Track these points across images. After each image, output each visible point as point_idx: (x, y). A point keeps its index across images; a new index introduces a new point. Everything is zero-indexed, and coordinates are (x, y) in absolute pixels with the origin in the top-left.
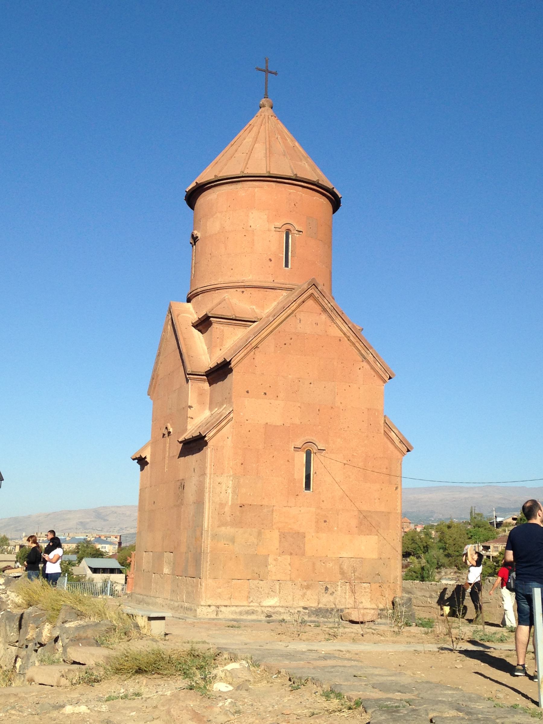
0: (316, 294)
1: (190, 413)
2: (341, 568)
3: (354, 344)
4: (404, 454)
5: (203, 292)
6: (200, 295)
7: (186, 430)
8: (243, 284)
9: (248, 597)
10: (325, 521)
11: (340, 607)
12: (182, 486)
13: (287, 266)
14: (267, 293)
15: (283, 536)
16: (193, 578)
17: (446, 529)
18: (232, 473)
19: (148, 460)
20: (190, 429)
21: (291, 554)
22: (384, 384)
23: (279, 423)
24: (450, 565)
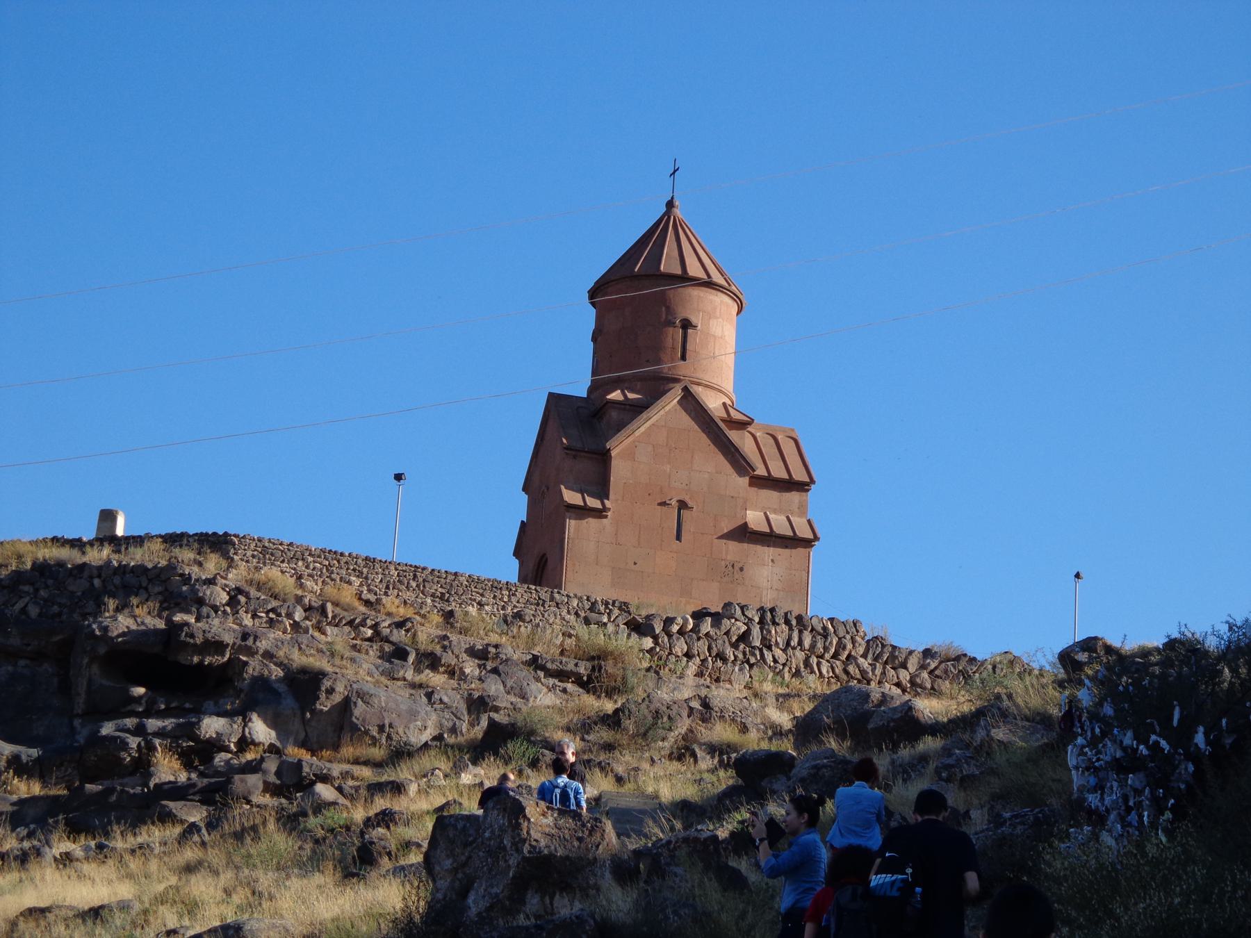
5: (707, 386)
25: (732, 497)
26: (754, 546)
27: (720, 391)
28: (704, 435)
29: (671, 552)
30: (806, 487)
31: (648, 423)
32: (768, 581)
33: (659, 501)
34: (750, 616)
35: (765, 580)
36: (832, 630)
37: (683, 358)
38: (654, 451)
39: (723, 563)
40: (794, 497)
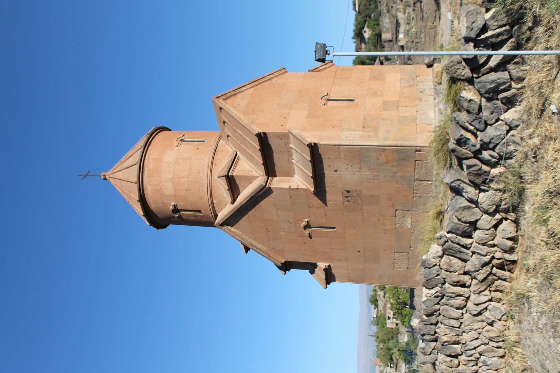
0: (223, 98)
1: (294, 186)
2: (408, 87)
3: (260, 83)
4: (334, 64)
5: (212, 198)
6: (214, 202)
7: (306, 190)
8: (210, 164)
9: (429, 124)
10: (376, 93)
11: (433, 86)
12: (348, 195)
13: (204, 141)
14: (219, 150)
15: (385, 109)
16: (416, 166)
17: (379, 339)
18: (339, 132)
19: (327, 264)
20: (306, 186)
21: (398, 106)
22: (288, 72)
23: (307, 112)
24: (397, 337)
25: (291, 197)
26: (326, 183)
27: (211, 183)
28: (250, 213)
29: (345, 233)
30: (262, 135)
31: (255, 245)
32: (354, 174)
33: (309, 238)
34: (431, 350)
35: (354, 176)
36: (438, 288)
37: (199, 211)
38: (272, 240)
39: (346, 203)
40: (273, 142)
